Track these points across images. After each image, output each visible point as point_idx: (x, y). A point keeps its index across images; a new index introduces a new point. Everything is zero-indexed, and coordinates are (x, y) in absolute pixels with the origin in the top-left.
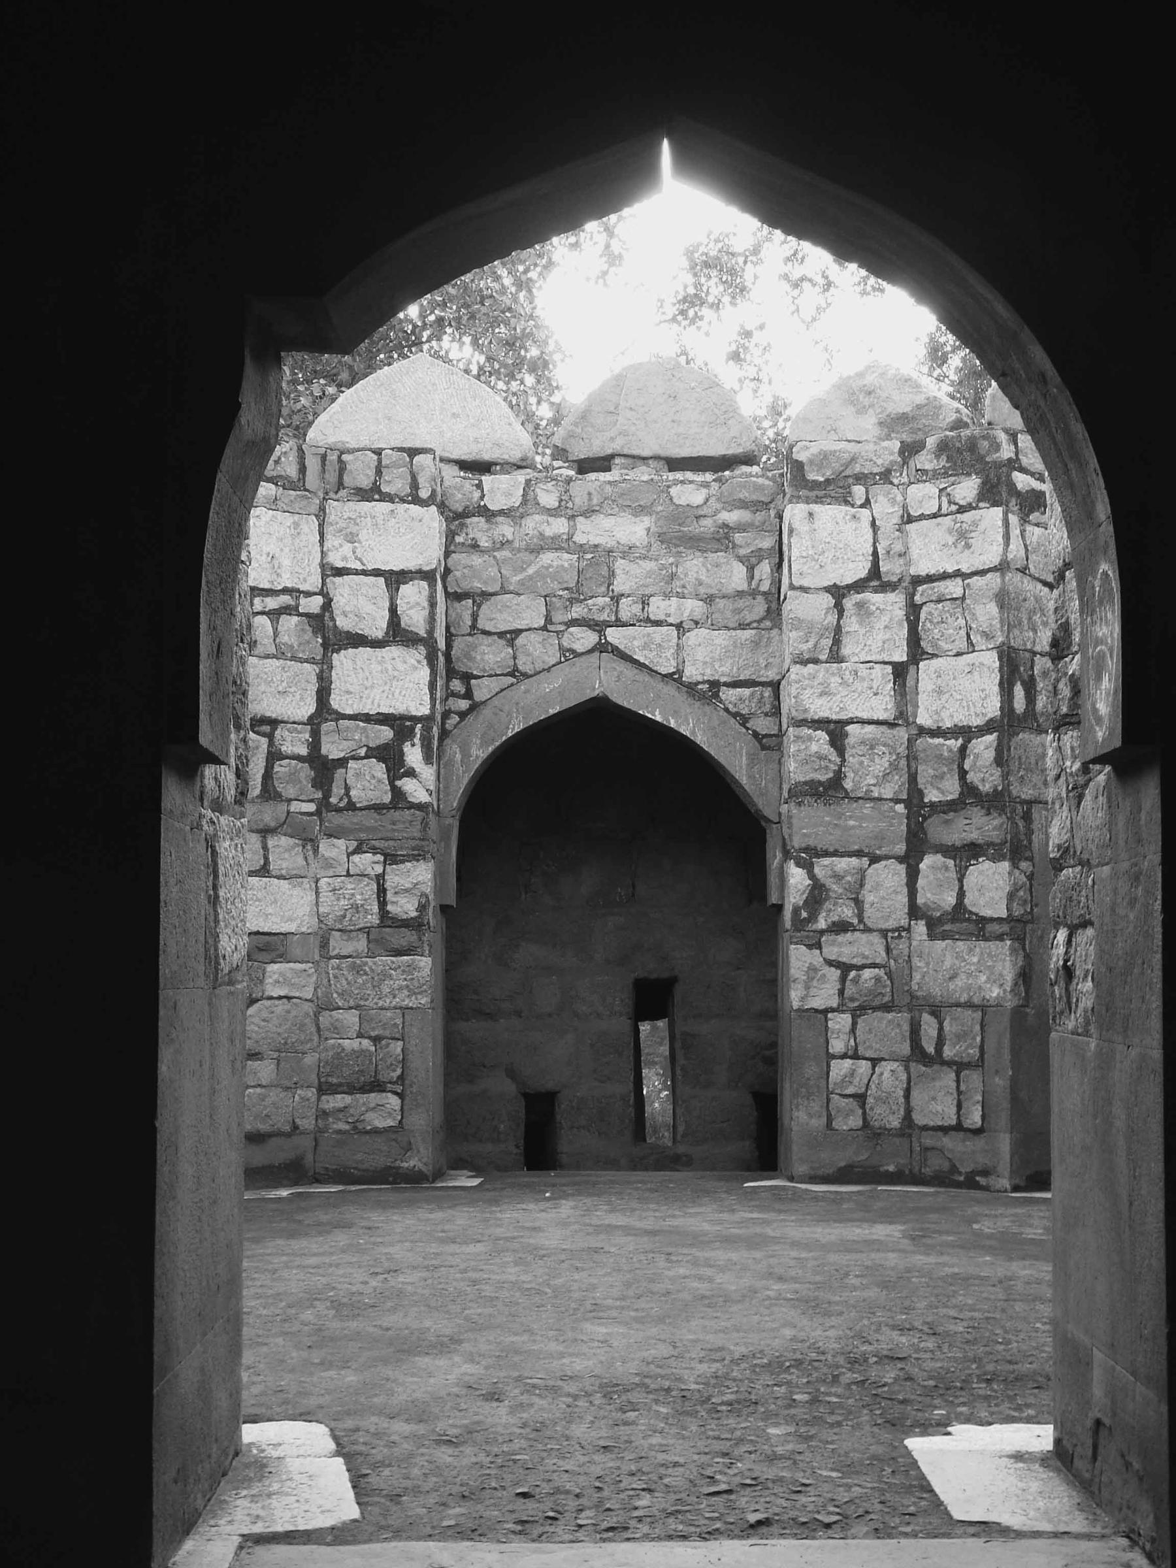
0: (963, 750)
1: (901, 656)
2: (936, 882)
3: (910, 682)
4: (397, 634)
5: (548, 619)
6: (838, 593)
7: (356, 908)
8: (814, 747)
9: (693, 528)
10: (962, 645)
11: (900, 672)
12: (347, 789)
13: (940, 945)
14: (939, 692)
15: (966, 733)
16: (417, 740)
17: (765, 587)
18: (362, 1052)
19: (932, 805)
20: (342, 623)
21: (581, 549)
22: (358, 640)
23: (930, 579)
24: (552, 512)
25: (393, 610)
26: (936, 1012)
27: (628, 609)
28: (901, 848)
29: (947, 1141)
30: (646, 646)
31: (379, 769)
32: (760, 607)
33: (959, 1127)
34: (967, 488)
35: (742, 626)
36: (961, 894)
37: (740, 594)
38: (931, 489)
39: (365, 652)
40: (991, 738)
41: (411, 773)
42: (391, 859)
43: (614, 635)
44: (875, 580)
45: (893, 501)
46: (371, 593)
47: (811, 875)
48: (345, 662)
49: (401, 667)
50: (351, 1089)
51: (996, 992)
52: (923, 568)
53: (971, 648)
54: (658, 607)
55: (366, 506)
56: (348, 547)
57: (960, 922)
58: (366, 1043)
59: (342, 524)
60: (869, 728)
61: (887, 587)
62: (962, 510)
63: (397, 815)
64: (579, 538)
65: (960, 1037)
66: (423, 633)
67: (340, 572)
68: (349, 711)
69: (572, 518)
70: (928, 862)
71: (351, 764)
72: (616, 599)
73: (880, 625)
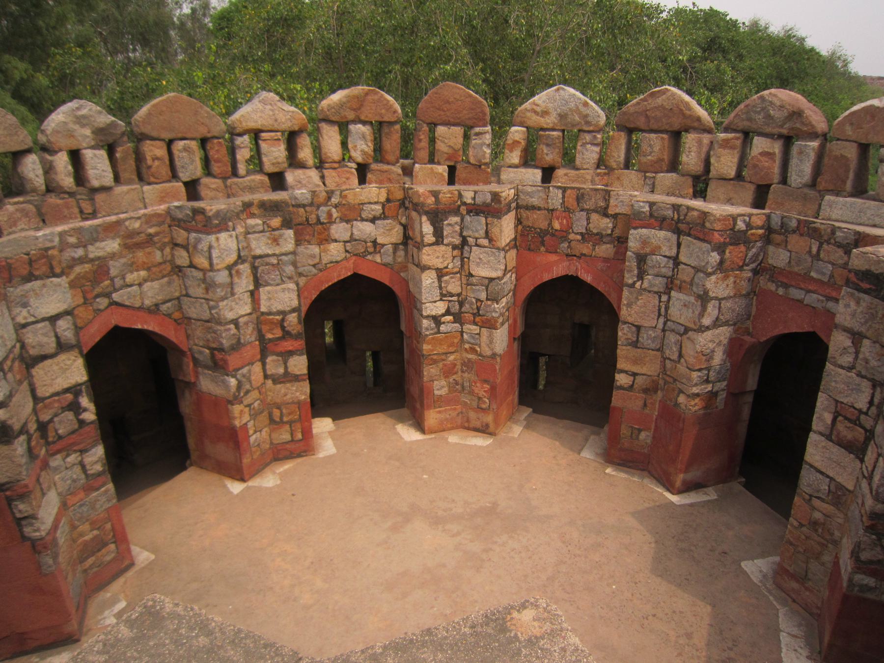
0: (283, 320)
1: (251, 288)
2: (274, 366)
3: (256, 297)
4: (62, 347)
5: (85, 298)
6: (229, 268)
7: (74, 481)
8: (232, 332)
9: (137, 239)
10: (280, 282)
11: (252, 293)
12: (56, 431)
13: (279, 386)
14: (270, 299)
15: (283, 313)
16: (84, 394)
17: (169, 258)
18: (96, 537)
19: (270, 339)
20: (32, 352)
21: (92, 260)
22: (44, 357)
23: (260, 257)
24: (75, 246)
25: (57, 337)
26: (279, 408)
27: (118, 282)
28: (259, 357)
29: (288, 446)
30: (129, 298)
31: (70, 415)
32: (168, 267)
33: (292, 441)
34: (276, 222)
35: (163, 277)
36: (286, 368)
37: (160, 264)
38: (259, 221)
39: (48, 362)
40: (295, 314)
41: (85, 410)
42: (82, 452)
43: (116, 297)
44: (240, 259)
45: (242, 227)
46: (44, 331)
47: (237, 379)
48: (38, 371)
49: (69, 362)
50: (93, 554)
51: (303, 397)
52: (258, 252)
53: (283, 282)
54: (130, 278)
55: (29, 285)
56: (24, 312)
57: (288, 377)
58: (96, 532)
59: (18, 300)
60: (246, 317)
61: (244, 262)
62: (274, 230)
63: (82, 431)
64: (91, 256)
65: (290, 414)
66: (74, 342)
67: (24, 326)
68: (48, 395)
69: (85, 246)
70: (269, 359)
71: (56, 419)
72: (112, 279)
73: (244, 277)
